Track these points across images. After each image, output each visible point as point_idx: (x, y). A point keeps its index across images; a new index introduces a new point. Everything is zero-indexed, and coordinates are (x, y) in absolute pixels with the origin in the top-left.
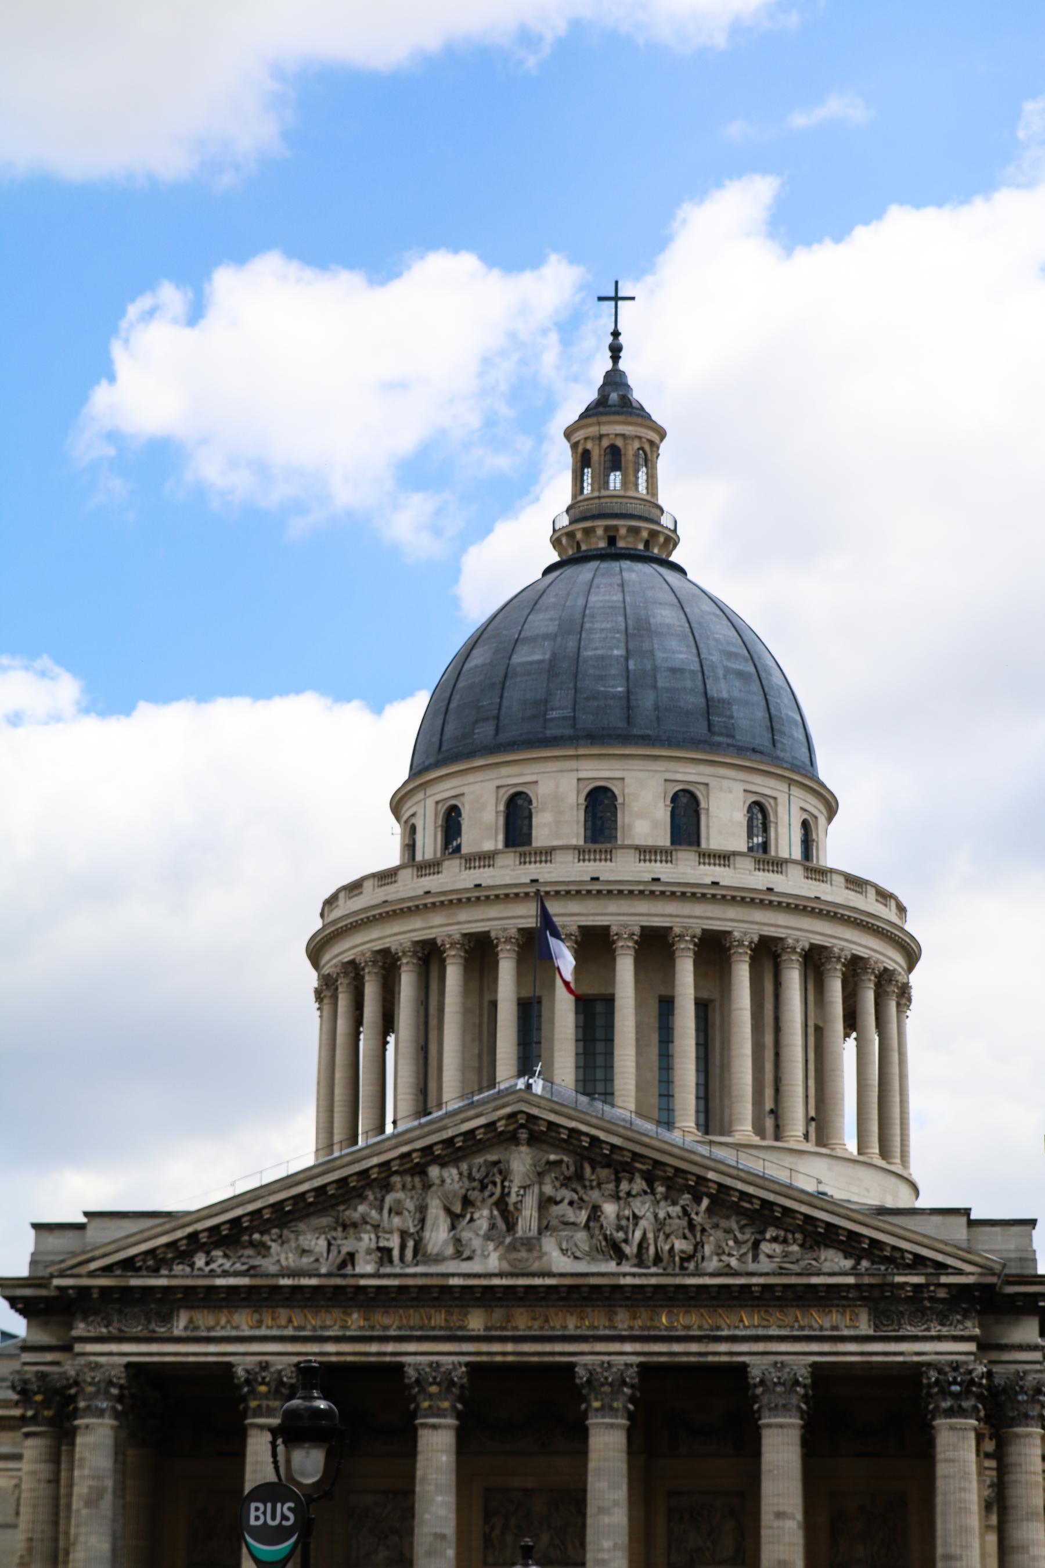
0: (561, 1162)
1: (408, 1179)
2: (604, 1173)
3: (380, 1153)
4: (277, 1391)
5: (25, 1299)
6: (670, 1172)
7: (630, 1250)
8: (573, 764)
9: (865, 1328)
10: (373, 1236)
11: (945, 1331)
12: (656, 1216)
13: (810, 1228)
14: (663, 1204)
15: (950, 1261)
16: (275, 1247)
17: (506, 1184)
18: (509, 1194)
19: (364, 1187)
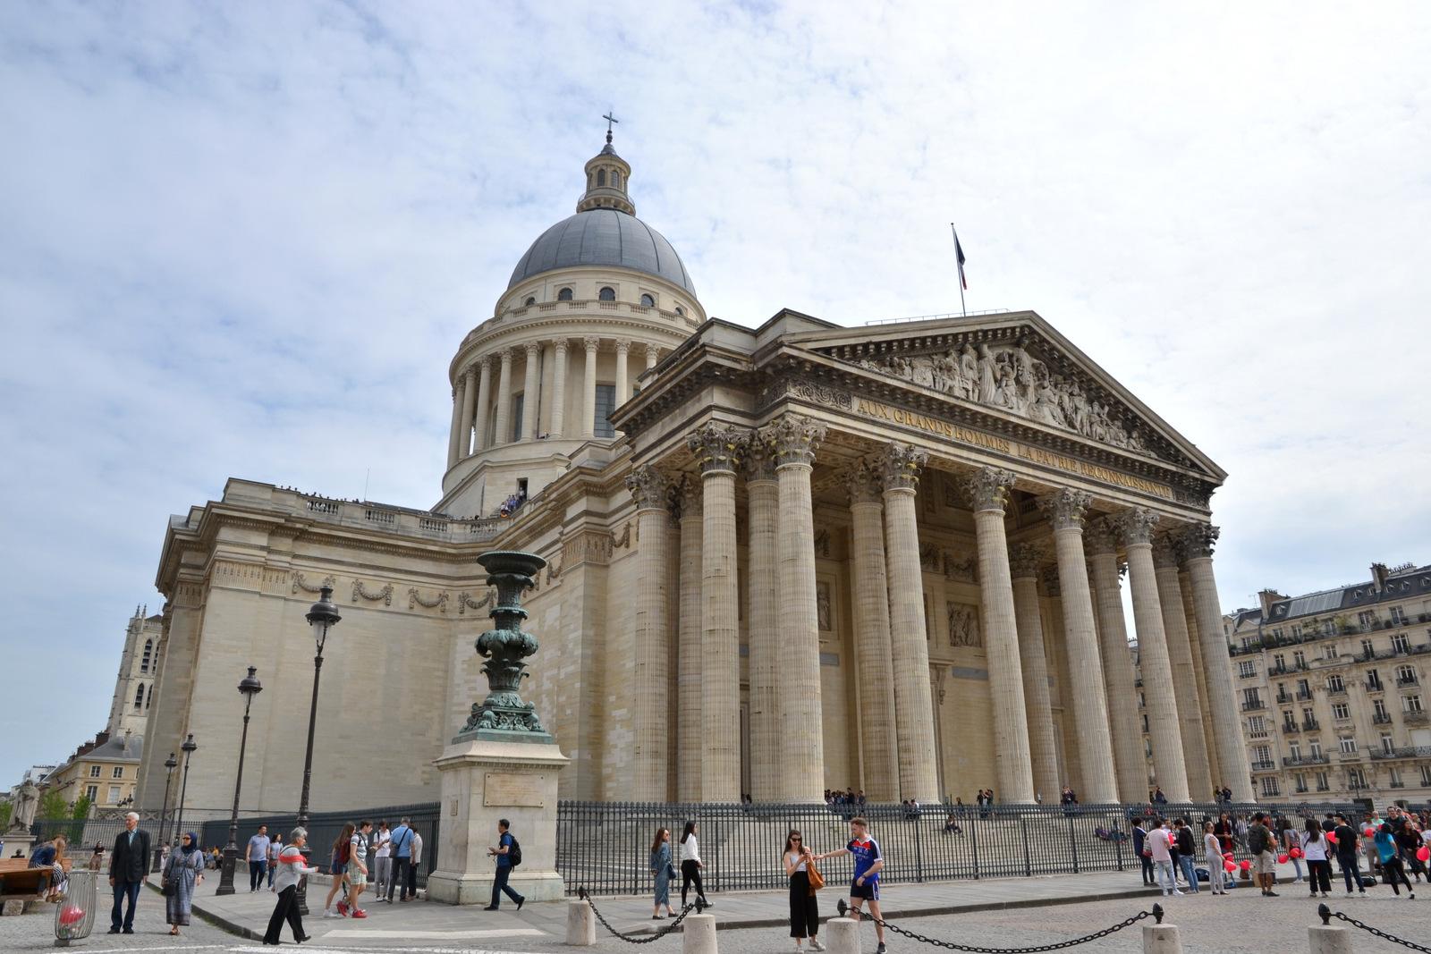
0: (1041, 364)
2: (1060, 378)
5: (721, 366)
6: (1094, 386)
7: (1078, 425)
8: (637, 280)
9: (1171, 499)
11: (1200, 508)
15: (1206, 469)
16: (908, 369)
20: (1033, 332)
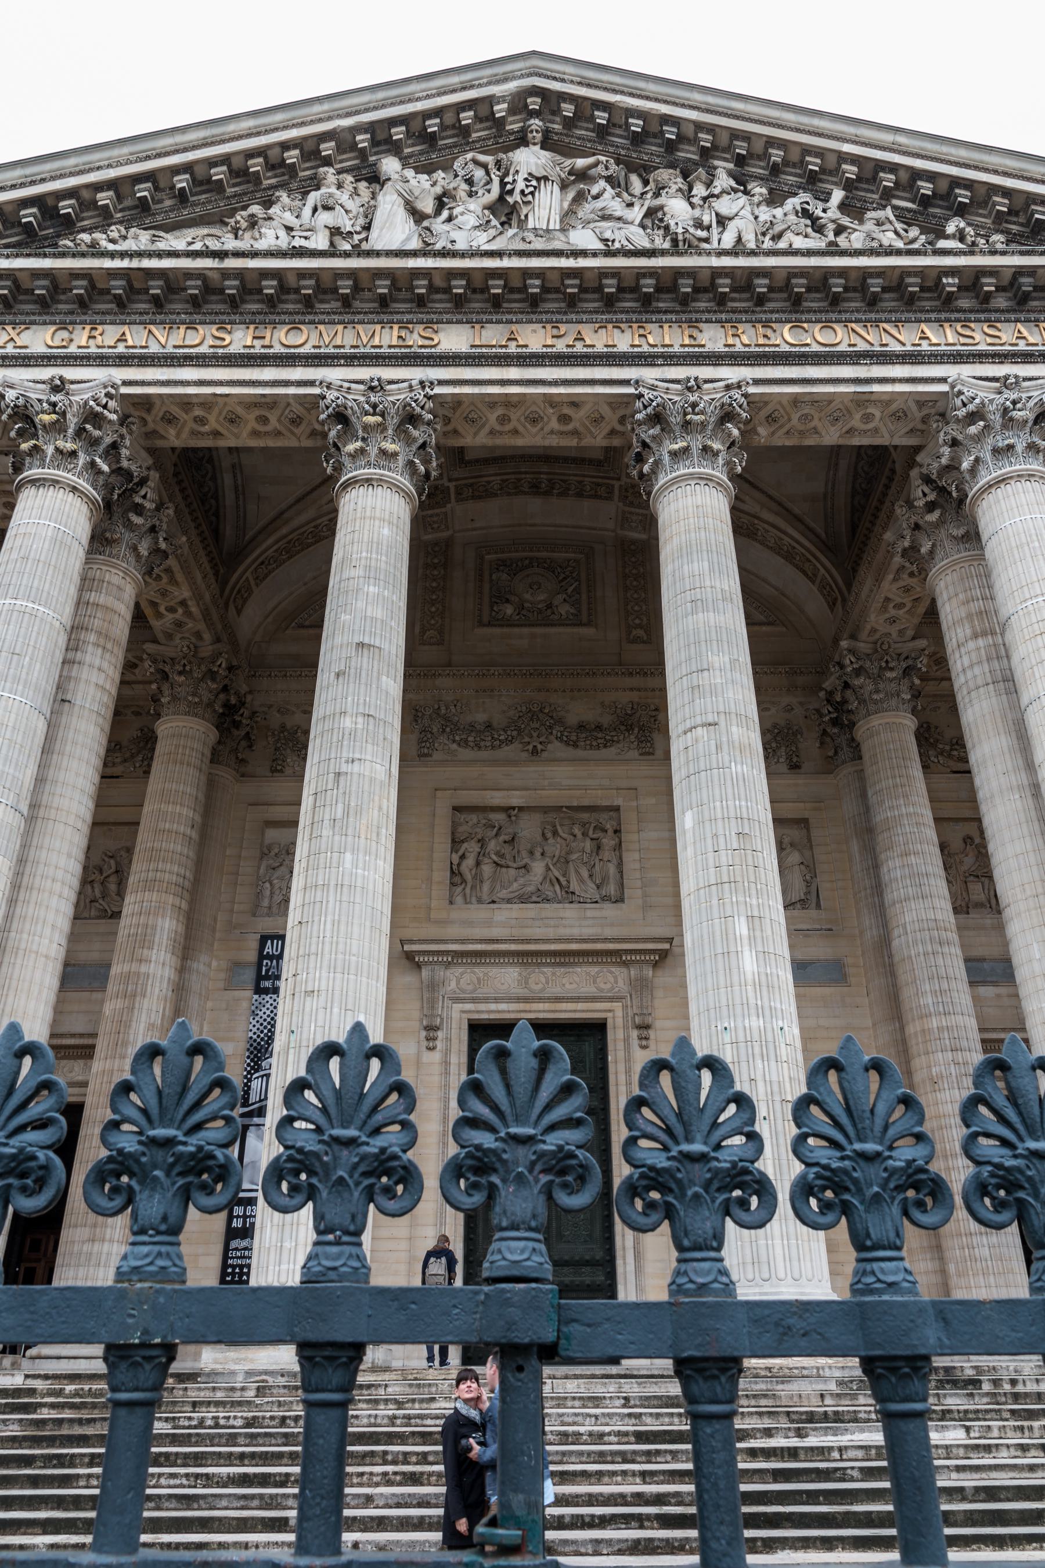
1: (349, 178)
2: (664, 174)
3: (303, 124)
4: (80, 432)
10: (282, 233)
12: (756, 218)
13: (1015, 228)
14: (763, 208)
17: (509, 179)
18: (511, 192)
19: (275, 187)
20: (551, 100)
